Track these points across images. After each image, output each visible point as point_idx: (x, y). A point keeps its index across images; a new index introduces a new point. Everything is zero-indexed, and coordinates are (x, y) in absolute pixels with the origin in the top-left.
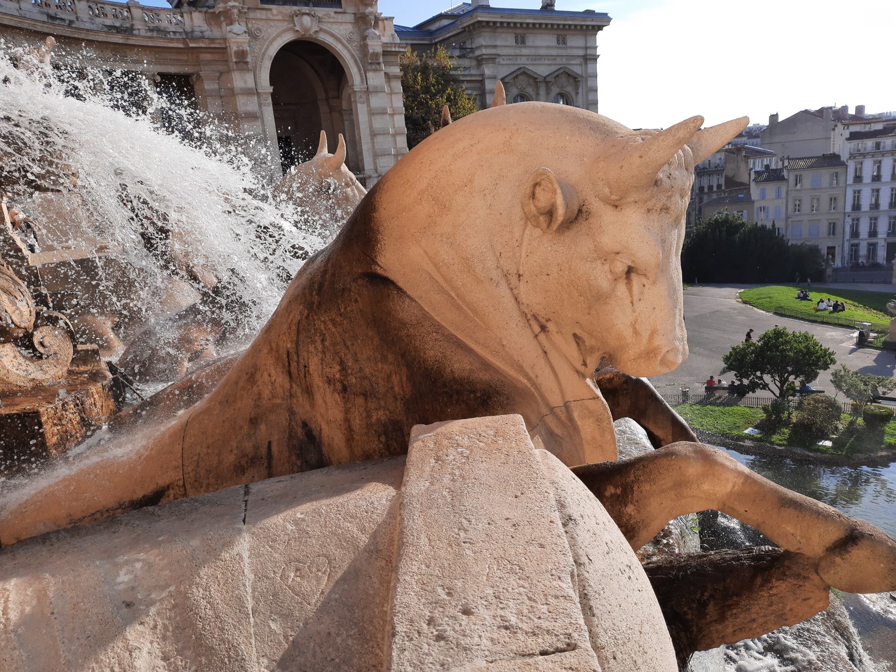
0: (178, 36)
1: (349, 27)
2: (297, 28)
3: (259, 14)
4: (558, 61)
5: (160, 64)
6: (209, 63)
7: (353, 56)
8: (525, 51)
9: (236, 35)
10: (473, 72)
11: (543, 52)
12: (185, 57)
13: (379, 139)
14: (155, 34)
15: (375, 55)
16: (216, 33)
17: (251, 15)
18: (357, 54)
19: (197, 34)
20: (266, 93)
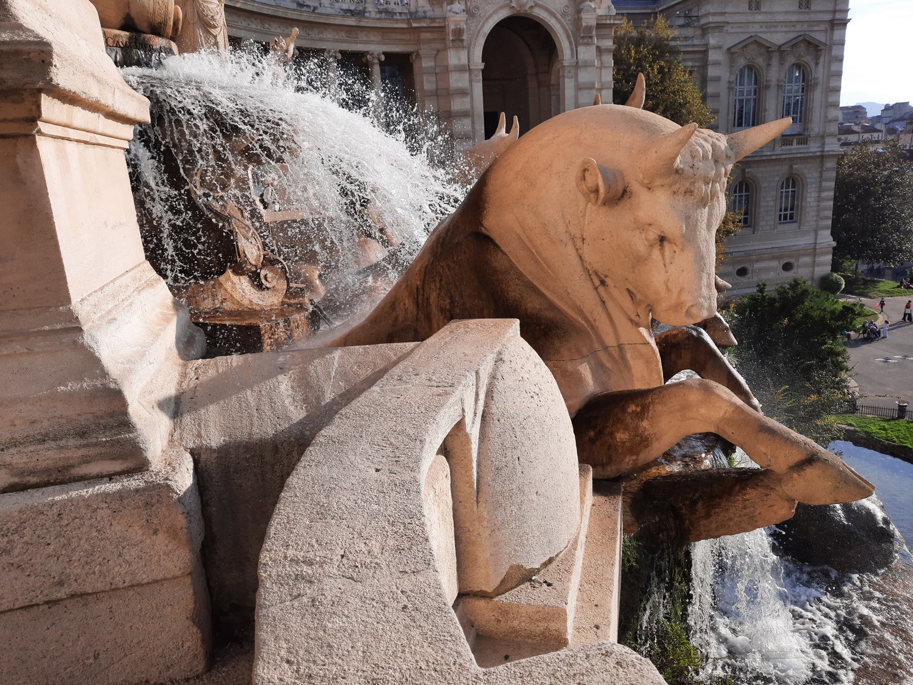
0: (403, 17)
2: (513, 4)
4: (798, 28)
5: (385, 44)
7: (565, 30)
8: (759, 18)
10: (696, 42)
11: (780, 18)
12: (407, 37)
14: (383, 15)
15: (589, 29)
16: (438, 12)
18: (569, 28)
19: (420, 14)
20: (477, 70)
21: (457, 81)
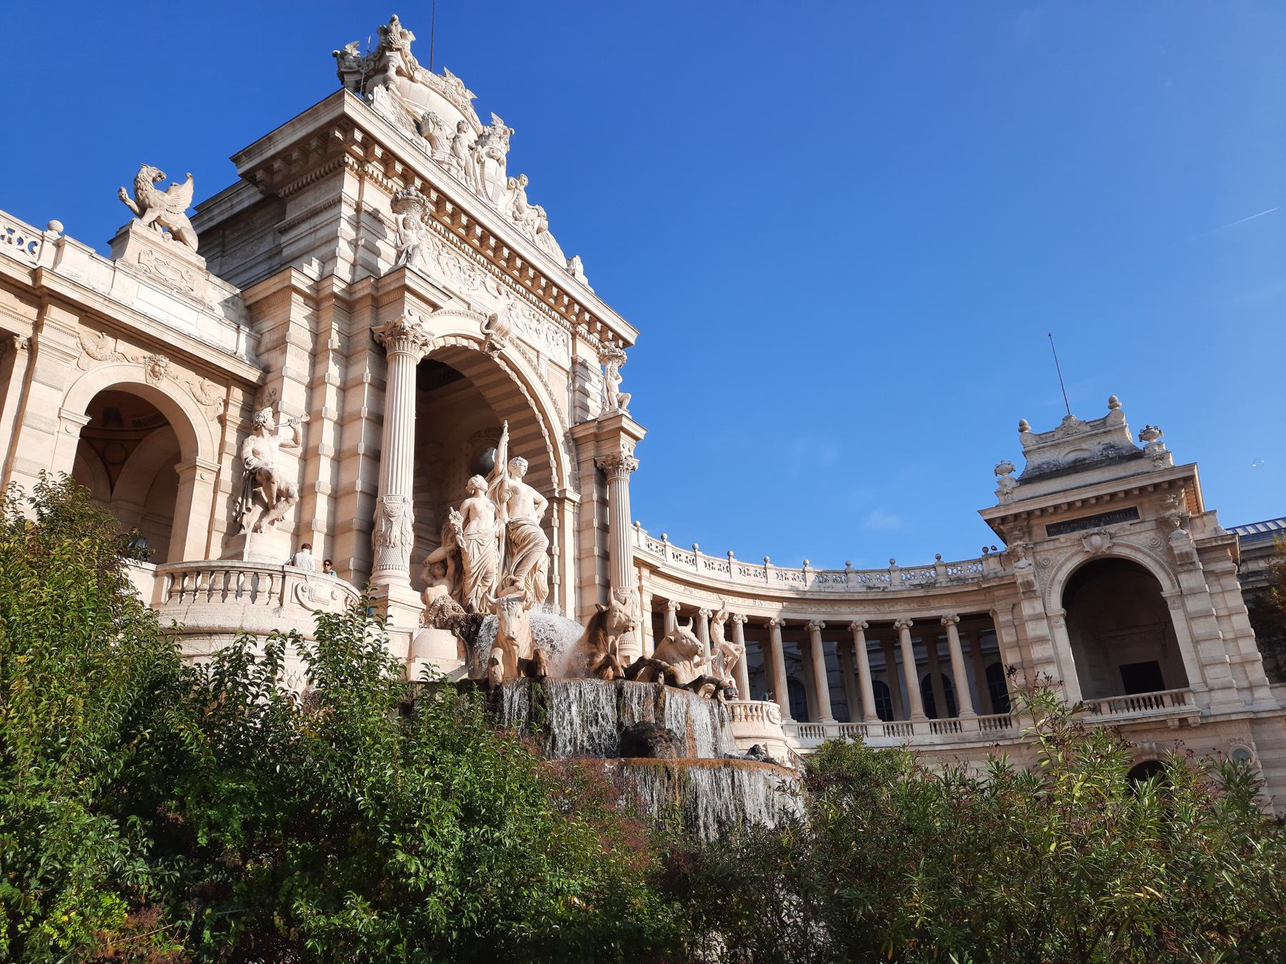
1: (1152, 534)
3: (1046, 546)
6: (1004, 598)
9: (1023, 569)
13: (1202, 647)
15: (1186, 556)
17: (1039, 548)
18: (1163, 559)
19: (992, 575)
21: (1033, 630)
